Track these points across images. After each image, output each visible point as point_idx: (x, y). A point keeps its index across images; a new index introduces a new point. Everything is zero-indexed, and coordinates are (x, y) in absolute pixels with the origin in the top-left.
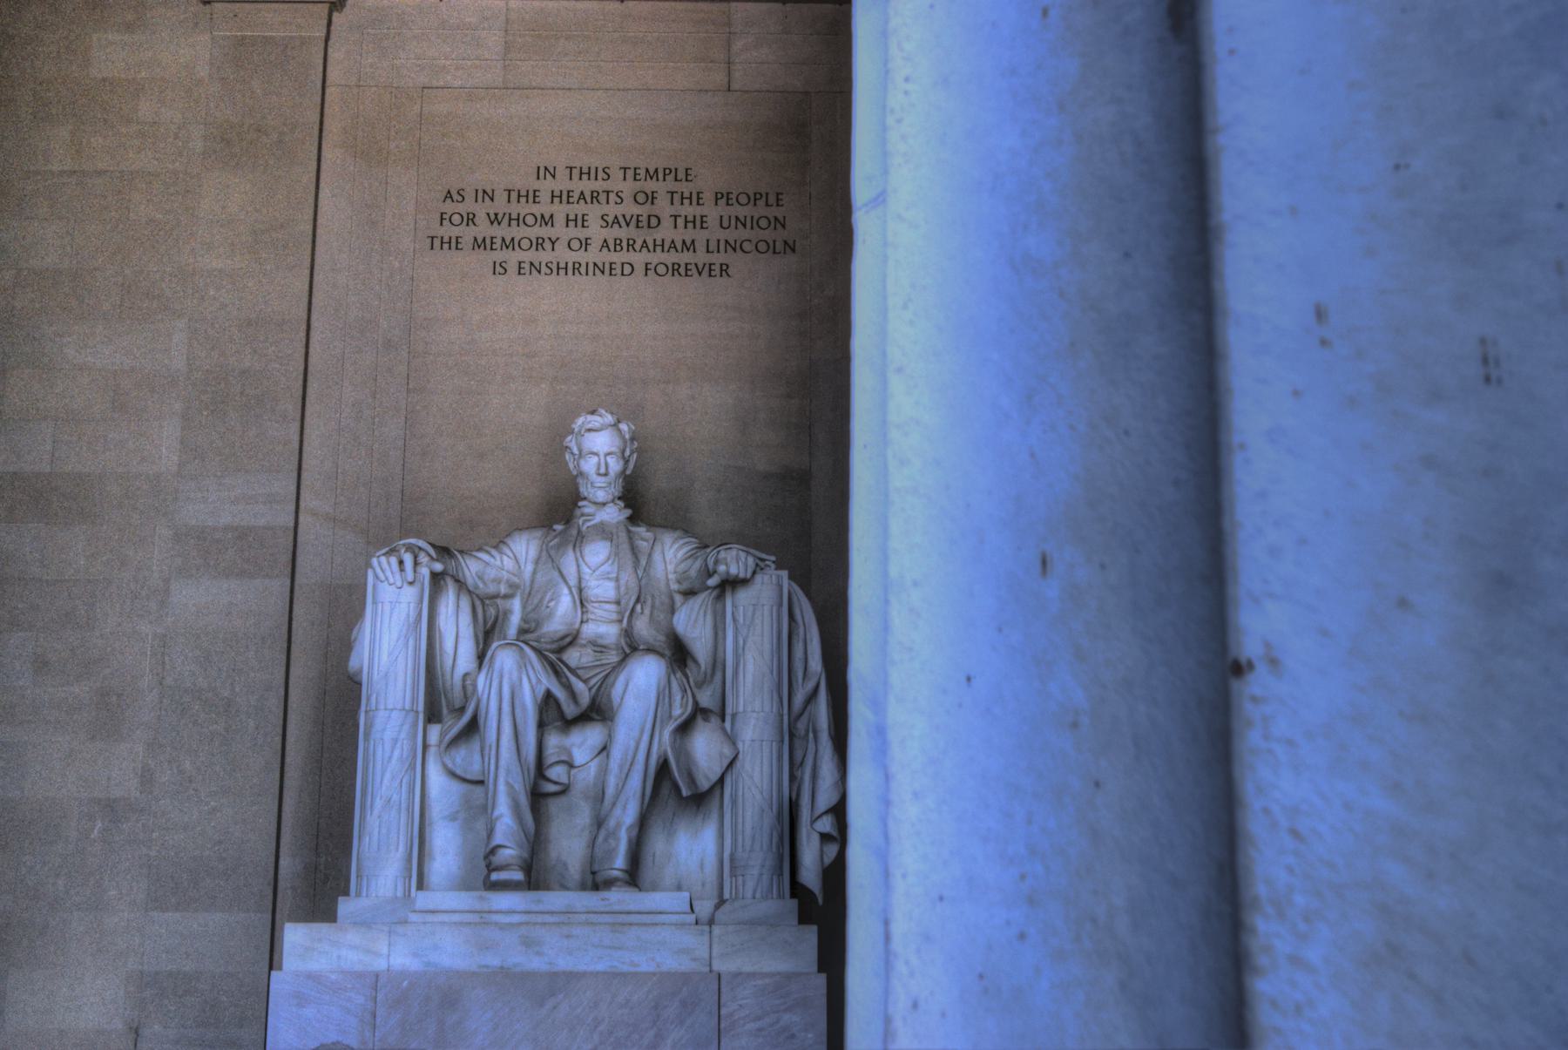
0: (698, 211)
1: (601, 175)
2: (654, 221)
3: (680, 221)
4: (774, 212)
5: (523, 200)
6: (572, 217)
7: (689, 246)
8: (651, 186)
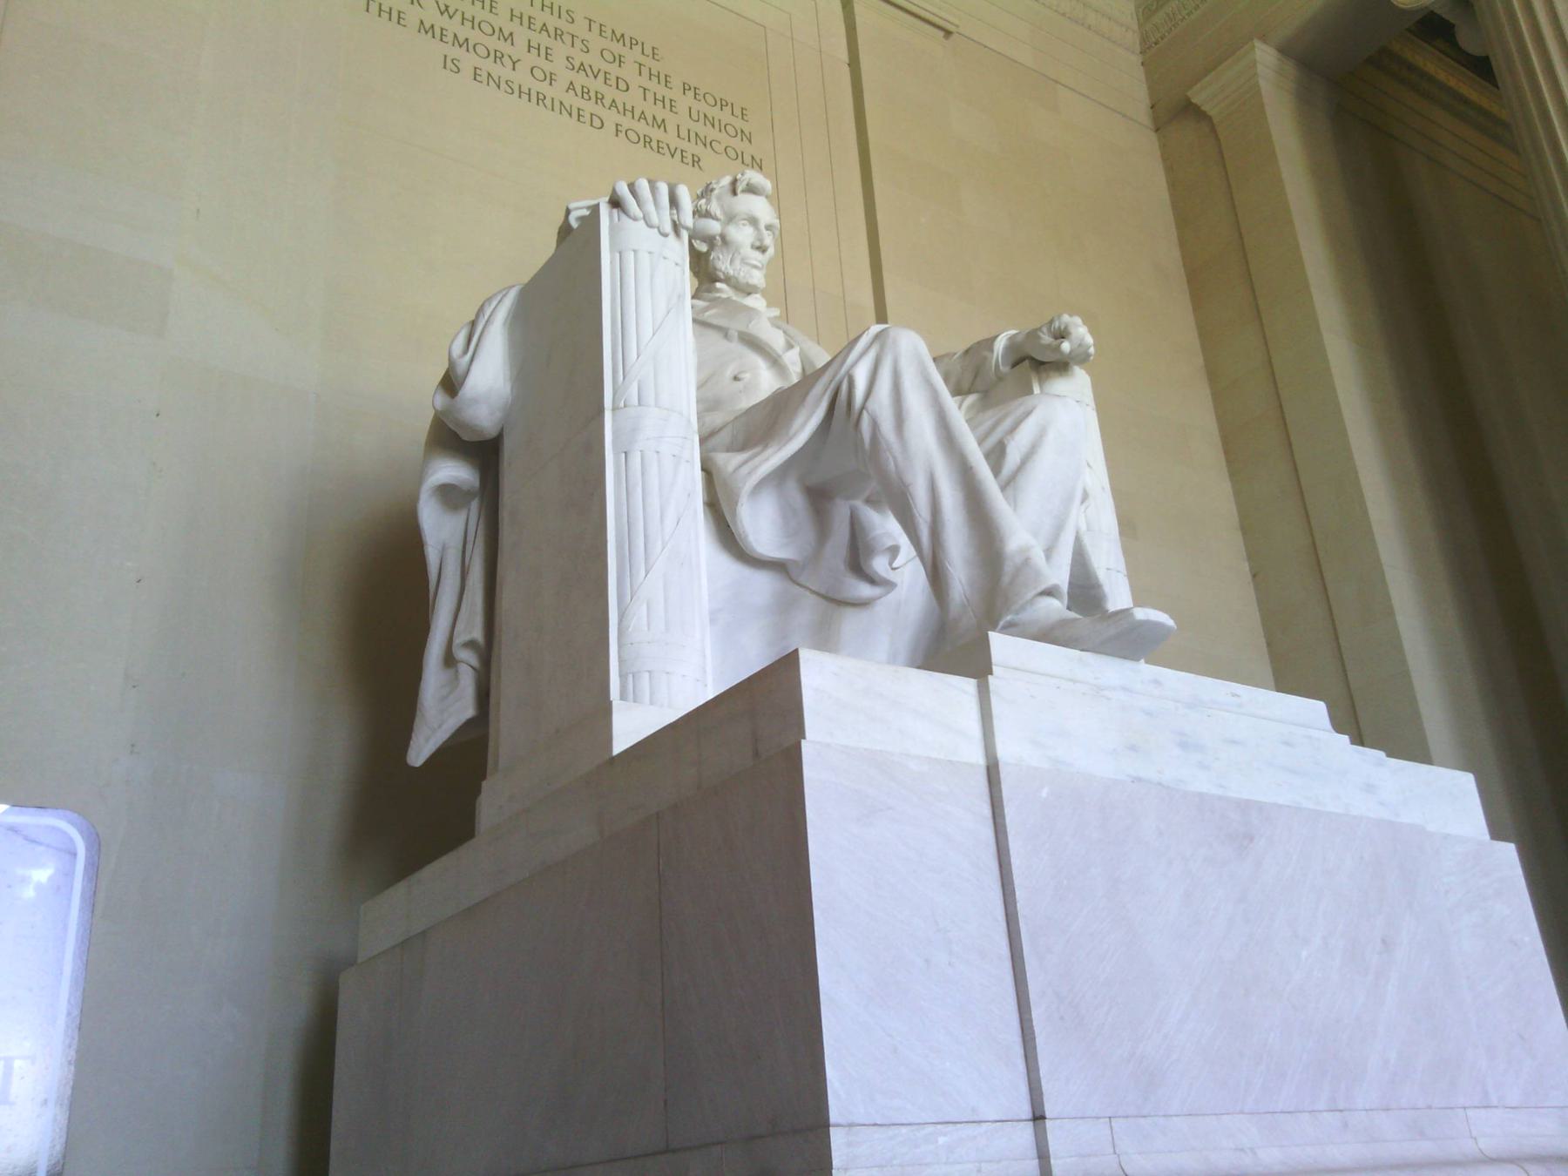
0: (669, 94)
2: (622, 86)
3: (650, 96)
4: (739, 124)
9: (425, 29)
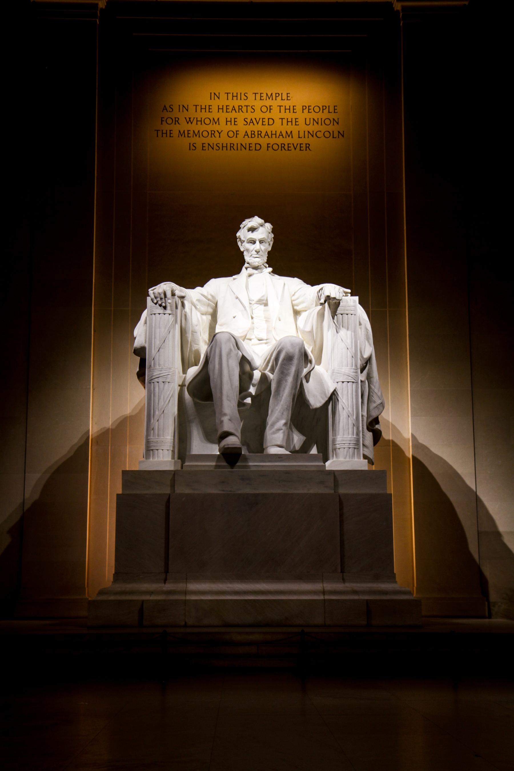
1: (243, 97)
2: (271, 122)
3: (285, 121)
4: (332, 116)
5: (203, 111)
6: (229, 119)
7: (290, 134)
8: (269, 102)
9: (181, 134)
